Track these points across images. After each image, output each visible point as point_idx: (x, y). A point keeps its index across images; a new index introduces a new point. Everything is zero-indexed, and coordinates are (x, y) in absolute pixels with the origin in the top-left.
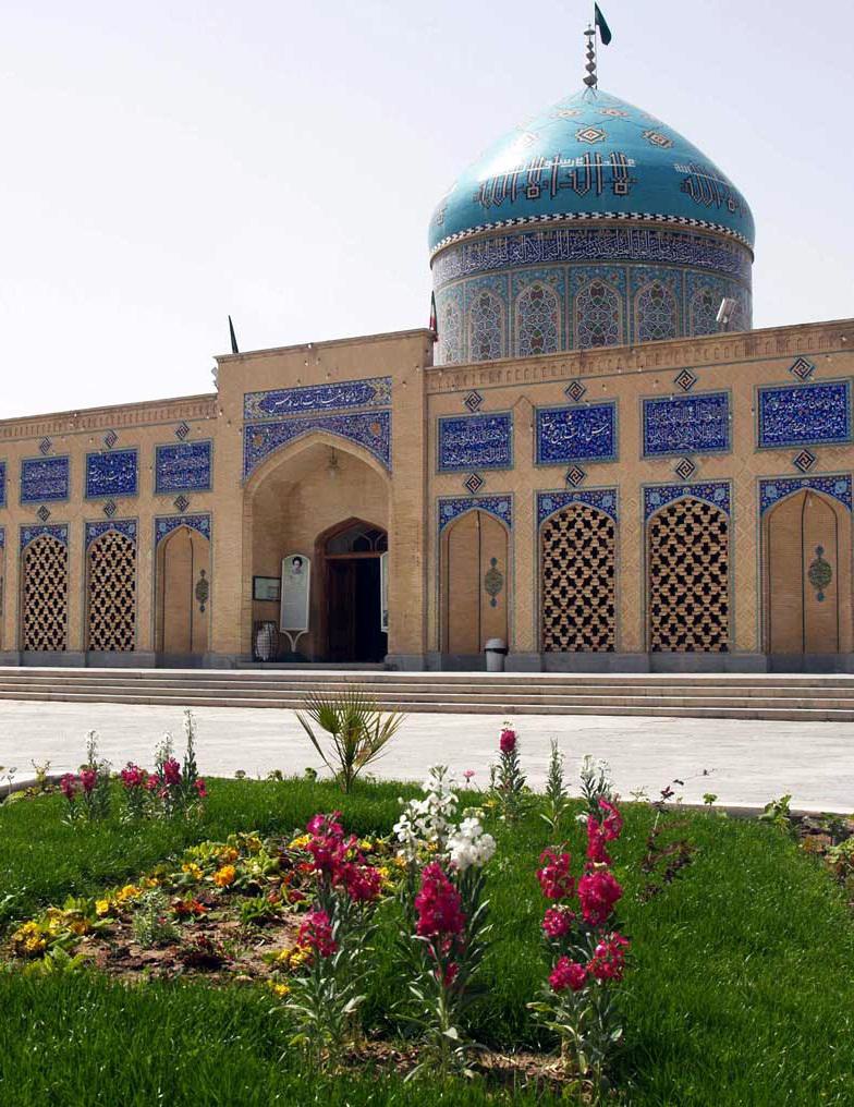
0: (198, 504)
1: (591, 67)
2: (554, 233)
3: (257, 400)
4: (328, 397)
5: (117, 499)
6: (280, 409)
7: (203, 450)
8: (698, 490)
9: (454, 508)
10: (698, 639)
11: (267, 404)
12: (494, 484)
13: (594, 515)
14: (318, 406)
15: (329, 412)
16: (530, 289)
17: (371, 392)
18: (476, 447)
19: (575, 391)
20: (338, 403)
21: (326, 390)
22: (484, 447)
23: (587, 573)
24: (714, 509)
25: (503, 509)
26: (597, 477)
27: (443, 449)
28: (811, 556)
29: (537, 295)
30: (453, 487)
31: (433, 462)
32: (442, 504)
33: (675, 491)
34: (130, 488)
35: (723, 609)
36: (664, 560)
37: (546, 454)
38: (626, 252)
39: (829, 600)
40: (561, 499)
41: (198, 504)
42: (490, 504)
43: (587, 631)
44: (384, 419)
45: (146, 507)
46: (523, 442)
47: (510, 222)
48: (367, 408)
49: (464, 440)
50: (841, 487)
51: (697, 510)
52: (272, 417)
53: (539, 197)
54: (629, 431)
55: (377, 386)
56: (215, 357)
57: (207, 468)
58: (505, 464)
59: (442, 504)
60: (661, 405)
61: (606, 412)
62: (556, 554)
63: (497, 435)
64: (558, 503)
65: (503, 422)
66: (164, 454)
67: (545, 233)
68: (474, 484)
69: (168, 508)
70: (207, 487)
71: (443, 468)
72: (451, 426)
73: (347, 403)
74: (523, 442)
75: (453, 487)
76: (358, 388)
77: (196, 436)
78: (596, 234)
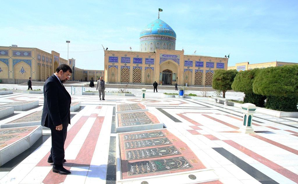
0: (152, 66)
5: (139, 64)
7: (153, 59)
8: (210, 71)
10: (138, 81)
11: (163, 55)
12: (191, 68)
15: (171, 58)
18: (189, 64)
19: (200, 60)
23: (199, 78)
24: (212, 73)
25: (191, 71)
26: (201, 69)
28: (148, 74)
30: (186, 68)
33: (209, 71)
34: (141, 63)
35: (201, 81)
36: (135, 74)
39: (187, 80)
40: (136, 67)
41: (152, 66)
42: (115, 66)
43: (199, 83)
45: (144, 65)
46: (194, 64)
48: (176, 58)
49: (187, 63)
52: (164, 57)
54: (205, 65)
57: (153, 62)
58: (192, 66)
60: (208, 63)
61: (203, 62)
62: (123, 72)
65: (192, 62)
66: (146, 59)
68: (188, 68)
70: (153, 64)
71: (185, 66)
74: (194, 64)
75: (186, 68)
76: (176, 56)
77: (152, 57)
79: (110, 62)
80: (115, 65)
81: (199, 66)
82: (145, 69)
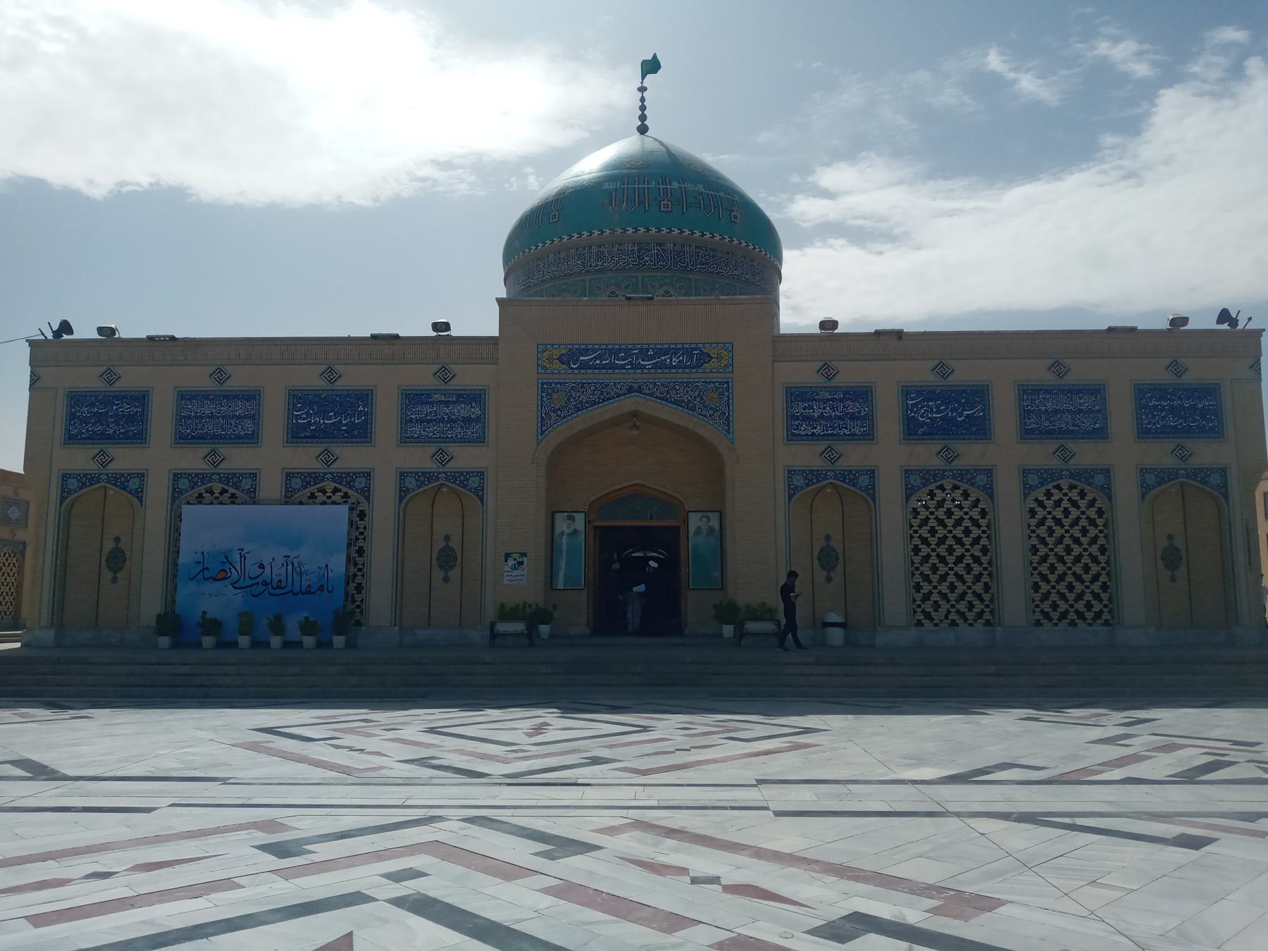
0: (465, 458)
3: (557, 354)
4: (650, 359)
6: (585, 366)
11: (569, 357)
14: (635, 367)
17: (705, 358)
20: (662, 366)
21: (647, 350)
30: (808, 456)
31: (781, 432)
32: (791, 473)
44: (724, 388)
50: (1215, 479)
51: (1074, 495)
55: (713, 353)
56: (497, 299)
59: (791, 473)
63: (852, 407)
66: (413, 398)
69: (419, 458)
70: (481, 440)
72: (796, 395)
73: (674, 367)
76: (689, 352)
79: (71, 439)
80: (116, 467)
81: (940, 430)
82: (403, 492)
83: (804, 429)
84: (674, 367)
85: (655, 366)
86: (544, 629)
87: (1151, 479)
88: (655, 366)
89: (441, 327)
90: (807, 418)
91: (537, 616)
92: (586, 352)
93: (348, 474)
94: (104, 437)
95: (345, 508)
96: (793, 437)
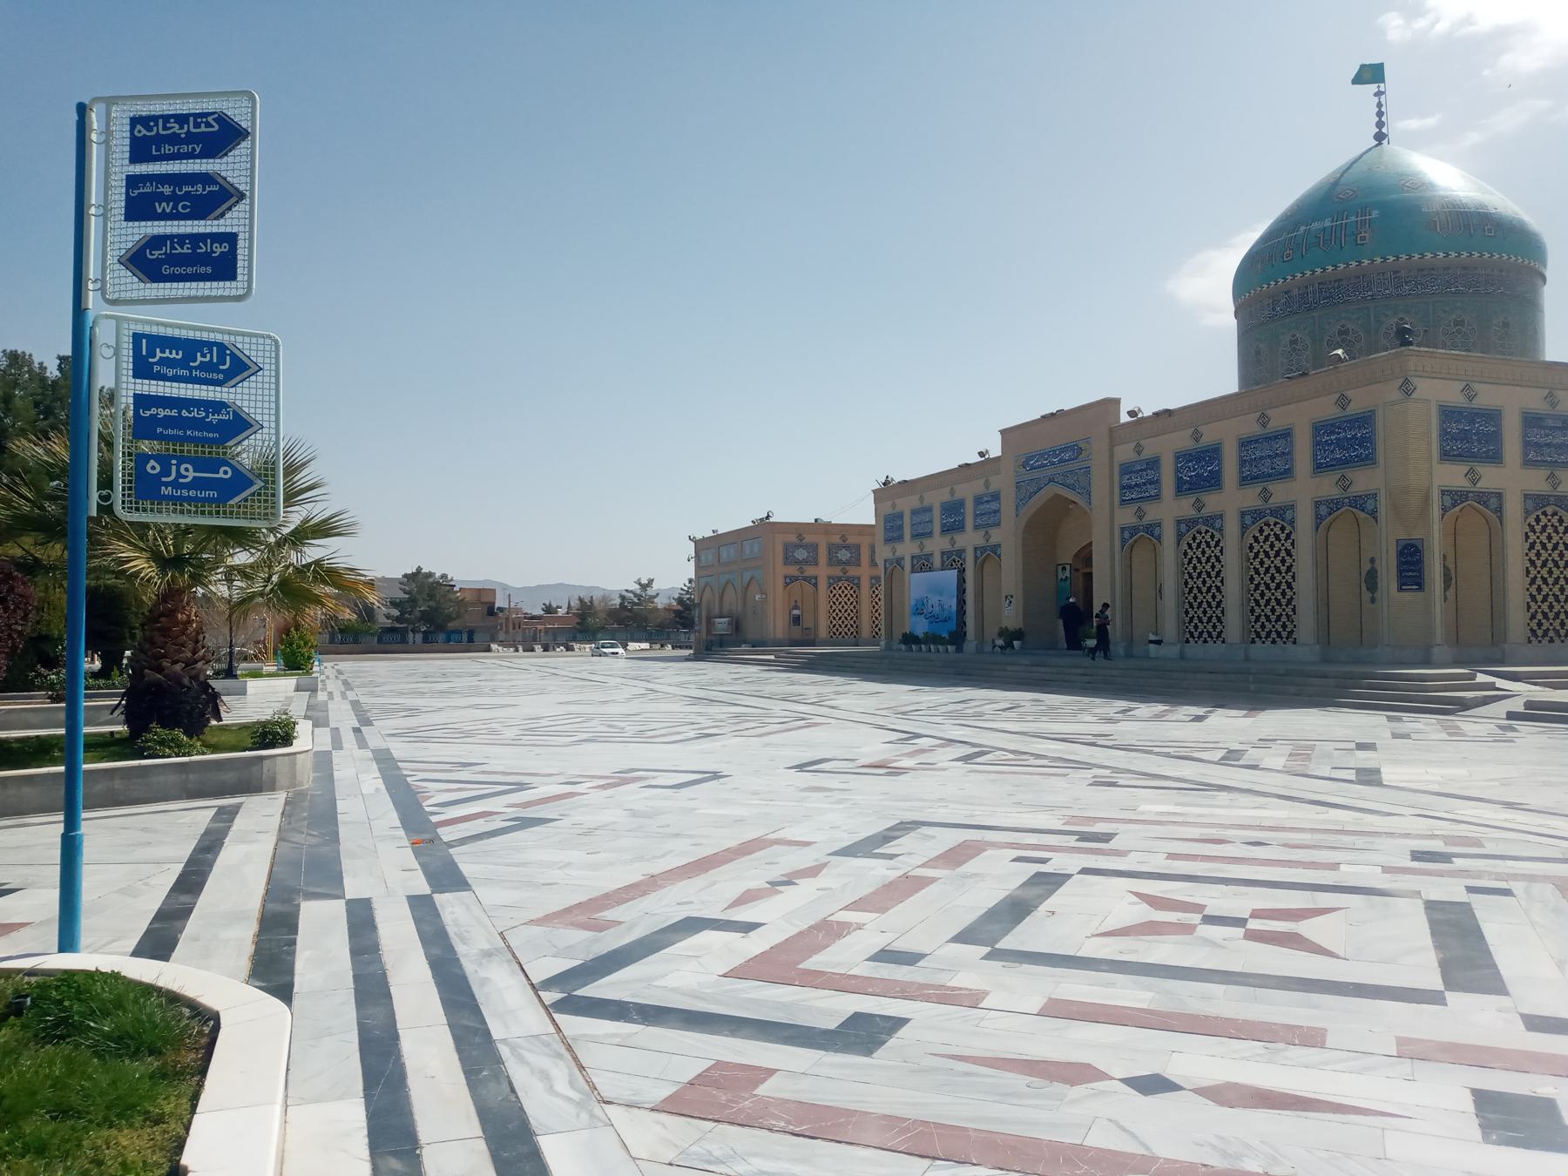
1: (1380, 124)
2: (1306, 287)
4: (1059, 455)
6: (1033, 468)
9: (1187, 526)
13: (1283, 529)
16: (1288, 338)
22: (1144, 484)
27: (1123, 487)
29: (1294, 342)
32: (1123, 530)
37: (1182, 488)
38: (1370, 293)
47: (1273, 283)
53: (1291, 260)
64: (1255, 519)
67: (1299, 288)
71: (1123, 502)
72: (1126, 469)
78: (1341, 283)
83: (1129, 496)
84: (1068, 461)
85: (1060, 462)
86: (1016, 643)
87: (1323, 510)
88: (1060, 462)
89: (981, 454)
90: (1130, 487)
91: (1019, 634)
92: (1032, 458)
93: (1281, 507)
94: (1345, 463)
95: (956, 571)
96: (1123, 502)
